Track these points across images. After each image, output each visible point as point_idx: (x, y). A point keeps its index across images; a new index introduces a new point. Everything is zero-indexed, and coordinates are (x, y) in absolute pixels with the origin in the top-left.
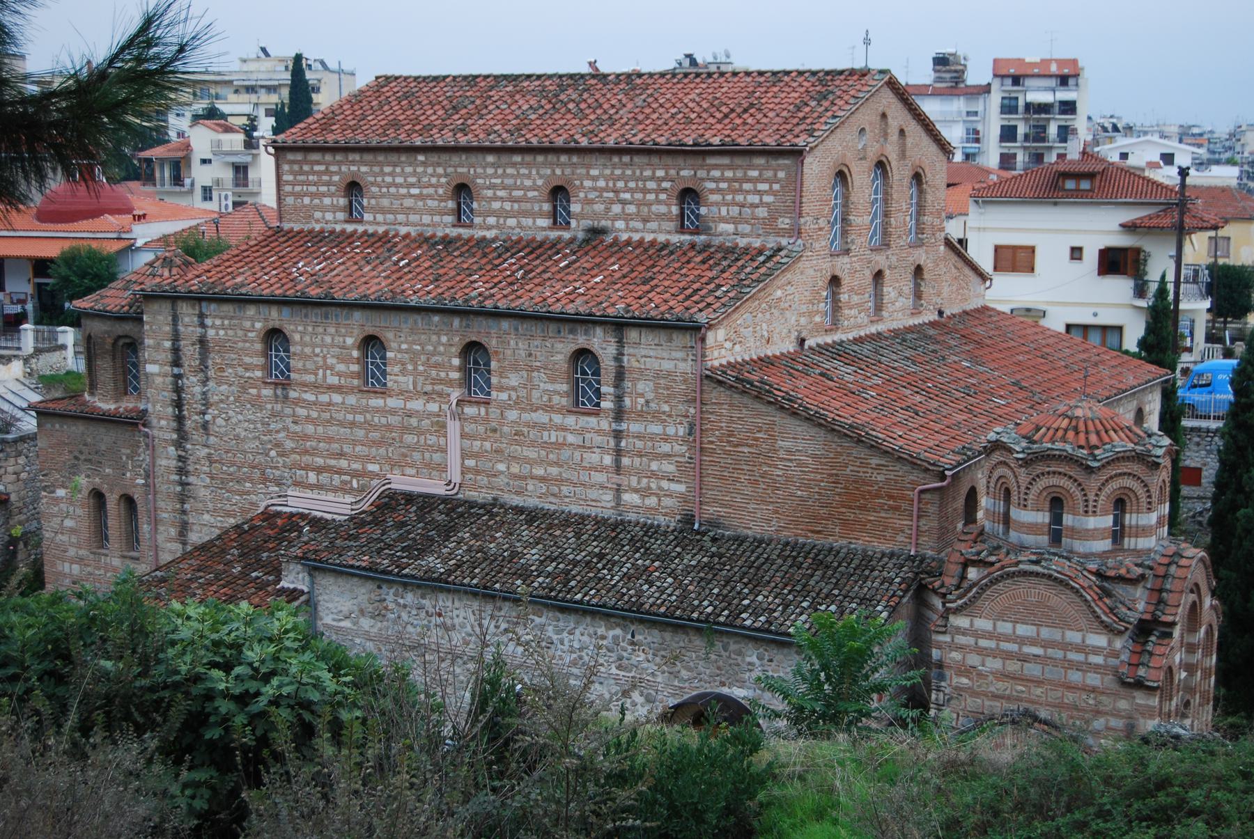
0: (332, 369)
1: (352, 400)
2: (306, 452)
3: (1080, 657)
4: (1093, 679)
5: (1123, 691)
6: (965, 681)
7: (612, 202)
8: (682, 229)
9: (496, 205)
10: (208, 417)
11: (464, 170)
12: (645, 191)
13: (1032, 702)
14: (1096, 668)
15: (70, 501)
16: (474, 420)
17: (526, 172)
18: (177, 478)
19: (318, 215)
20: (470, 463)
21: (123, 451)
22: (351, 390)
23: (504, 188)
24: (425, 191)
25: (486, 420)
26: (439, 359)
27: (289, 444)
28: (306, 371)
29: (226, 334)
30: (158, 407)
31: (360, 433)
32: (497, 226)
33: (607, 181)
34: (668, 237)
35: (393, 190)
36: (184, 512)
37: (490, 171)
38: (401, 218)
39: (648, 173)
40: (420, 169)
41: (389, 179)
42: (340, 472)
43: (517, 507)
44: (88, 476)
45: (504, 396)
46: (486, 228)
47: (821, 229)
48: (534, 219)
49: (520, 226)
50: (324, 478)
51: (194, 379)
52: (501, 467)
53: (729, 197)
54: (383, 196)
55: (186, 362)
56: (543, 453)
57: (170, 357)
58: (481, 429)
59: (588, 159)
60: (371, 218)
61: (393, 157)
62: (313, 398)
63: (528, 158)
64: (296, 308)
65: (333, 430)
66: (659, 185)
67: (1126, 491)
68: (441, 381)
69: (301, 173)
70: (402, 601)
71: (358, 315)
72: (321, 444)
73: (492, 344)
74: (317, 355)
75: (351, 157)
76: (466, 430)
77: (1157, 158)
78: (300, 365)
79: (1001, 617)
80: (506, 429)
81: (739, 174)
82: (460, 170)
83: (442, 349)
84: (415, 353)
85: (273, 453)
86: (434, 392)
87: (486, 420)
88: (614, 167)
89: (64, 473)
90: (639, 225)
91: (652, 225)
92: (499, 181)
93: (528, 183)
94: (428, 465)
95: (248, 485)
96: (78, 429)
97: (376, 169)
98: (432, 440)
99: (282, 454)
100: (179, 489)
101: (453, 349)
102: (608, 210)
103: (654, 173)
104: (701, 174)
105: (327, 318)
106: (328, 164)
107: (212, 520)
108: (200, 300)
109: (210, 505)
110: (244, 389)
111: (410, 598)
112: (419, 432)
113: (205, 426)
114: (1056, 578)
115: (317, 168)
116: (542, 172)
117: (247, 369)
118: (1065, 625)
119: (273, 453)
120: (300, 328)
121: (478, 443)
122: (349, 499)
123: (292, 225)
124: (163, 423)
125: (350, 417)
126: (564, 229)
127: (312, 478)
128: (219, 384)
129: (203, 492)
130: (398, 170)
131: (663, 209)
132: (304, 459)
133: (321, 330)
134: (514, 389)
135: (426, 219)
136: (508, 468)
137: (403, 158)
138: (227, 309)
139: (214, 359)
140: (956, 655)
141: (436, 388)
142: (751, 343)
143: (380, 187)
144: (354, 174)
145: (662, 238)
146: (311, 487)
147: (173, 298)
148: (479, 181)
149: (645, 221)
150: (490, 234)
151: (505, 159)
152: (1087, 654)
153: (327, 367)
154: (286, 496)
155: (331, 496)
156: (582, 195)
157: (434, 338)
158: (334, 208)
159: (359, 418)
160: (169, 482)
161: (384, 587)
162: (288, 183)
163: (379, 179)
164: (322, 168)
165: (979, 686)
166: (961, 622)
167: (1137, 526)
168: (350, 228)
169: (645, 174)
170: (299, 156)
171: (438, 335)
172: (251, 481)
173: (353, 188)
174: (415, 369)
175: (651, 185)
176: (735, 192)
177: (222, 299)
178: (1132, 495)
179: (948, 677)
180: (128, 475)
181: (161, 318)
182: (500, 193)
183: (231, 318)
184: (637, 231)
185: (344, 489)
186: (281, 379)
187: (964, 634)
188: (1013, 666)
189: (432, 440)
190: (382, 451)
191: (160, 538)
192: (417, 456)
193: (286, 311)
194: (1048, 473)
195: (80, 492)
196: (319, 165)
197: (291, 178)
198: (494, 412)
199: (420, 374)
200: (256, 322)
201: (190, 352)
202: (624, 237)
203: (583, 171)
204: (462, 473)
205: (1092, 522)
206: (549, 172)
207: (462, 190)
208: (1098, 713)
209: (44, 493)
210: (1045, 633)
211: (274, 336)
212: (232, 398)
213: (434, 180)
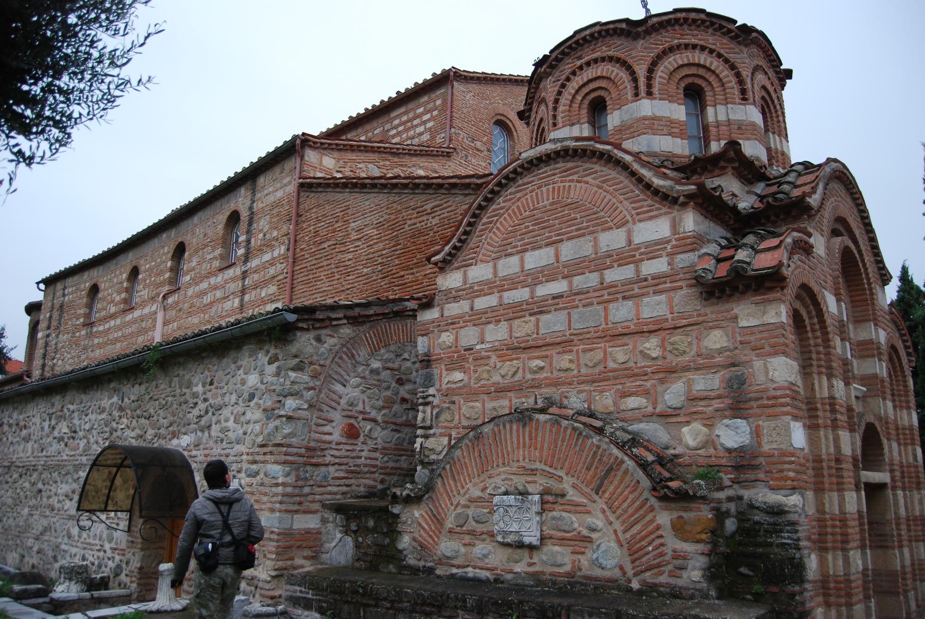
3: (628, 272)
4: (654, 307)
5: (711, 312)
6: (458, 376)
13: (556, 384)
14: (656, 283)
47: (478, 150)
53: (404, 136)
67: (701, 72)
79: (504, 251)
81: (411, 115)
104: (388, 126)
114: (575, 151)
118: (597, 223)
140: (446, 338)
152: (637, 263)
165: (479, 379)
166: (451, 280)
167: (729, 122)
176: (407, 130)
178: (712, 79)
179: (436, 377)
187: (456, 299)
188: (524, 328)
194: (581, 68)
205: (646, 107)
208: (670, 372)
210: (569, 251)
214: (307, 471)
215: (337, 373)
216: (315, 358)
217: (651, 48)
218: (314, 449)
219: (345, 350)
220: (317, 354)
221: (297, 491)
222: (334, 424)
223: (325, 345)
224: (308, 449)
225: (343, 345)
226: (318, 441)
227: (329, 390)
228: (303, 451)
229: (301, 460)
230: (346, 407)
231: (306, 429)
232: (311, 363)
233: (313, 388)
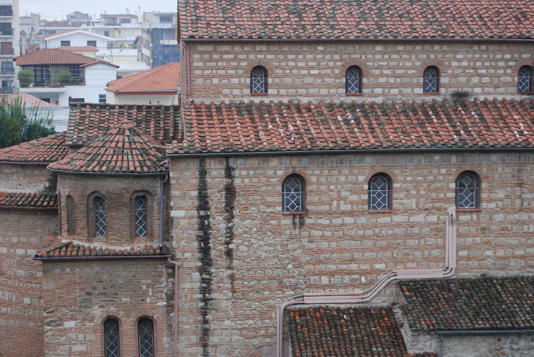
0: (345, 199)
1: (363, 220)
2: (321, 262)
7: (472, 76)
8: (520, 92)
9: (382, 80)
10: (231, 246)
11: (358, 56)
12: (496, 68)
15: (79, 330)
16: (467, 224)
17: (408, 57)
18: (201, 296)
19: (226, 91)
20: (464, 253)
21: (143, 281)
22: (363, 213)
23: (389, 68)
24: (323, 72)
25: (478, 222)
26: (438, 185)
27: (304, 259)
28: (322, 203)
29: (251, 181)
30: (183, 243)
31: (369, 243)
32: (383, 95)
33: (469, 60)
34: (513, 97)
35: (295, 71)
36: (206, 322)
37: (378, 57)
38: (301, 91)
39: (499, 56)
40: (319, 56)
41: (292, 64)
42: (350, 273)
43: (502, 277)
44: (103, 307)
45: (493, 205)
46: (373, 95)
48: (413, 88)
49: (401, 93)
50: (336, 279)
51: (221, 218)
52: (489, 253)
54: (287, 76)
55: (213, 205)
56: (523, 240)
57: (196, 203)
58: (473, 229)
59: (455, 48)
60: (275, 92)
61: (298, 48)
62: (328, 222)
63: (409, 48)
64: (313, 158)
65: (344, 244)
66: (506, 64)
68: (440, 200)
69: (211, 60)
70: (515, 347)
71: (369, 160)
72: (334, 255)
73: (483, 171)
74: (332, 191)
75: (258, 48)
76: (460, 231)
77: (85, 44)
78: (316, 199)
80: (493, 227)
82: (353, 56)
83: (441, 178)
84: (418, 182)
85: (290, 266)
86: (433, 208)
87: (478, 222)
88: (475, 52)
89: (73, 307)
90: (492, 90)
91: (502, 90)
92: (385, 63)
93: (408, 64)
94: (427, 259)
95: (266, 293)
96: (96, 268)
97: (281, 57)
98: (431, 241)
99: (299, 266)
100: (202, 304)
101: (451, 177)
102: (469, 81)
103: (503, 56)
105: (341, 163)
106: (236, 54)
107: (233, 324)
108: (227, 157)
109: (232, 313)
110: (265, 221)
111: (522, 343)
112: (420, 237)
113: (229, 253)
115: (225, 56)
116: (420, 56)
117: (268, 206)
119: (290, 266)
120: (316, 172)
121: (471, 239)
122: (357, 291)
123: (202, 100)
124: (187, 255)
125: (361, 233)
126: (436, 95)
127: (325, 280)
128: (242, 220)
129: (225, 304)
130: (301, 57)
131: (509, 79)
132: (318, 267)
133: (336, 172)
134: (501, 200)
135: (324, 91)
136: (495, 253)
137: (305, 48)
138: (254, 162)
139: (239, 201)
141: (436, 205)
143: (283, 69)
144: (260, 60)
145: (509, 98)
146: (324, 287)
147: (202, 157)
148: (368, 64)
149: (496, 87)
150: (379, 100)
151: (390, 48)
153: (340, 198)
154: (303, 296)
155: (342, 291)
156: (450, 71)
157: (435, 171)
158: (241, 86)
159: (369, 232)
160: (192, 300)
161: (503, 339)
162: (197, 68)
163: (283, 64)
164: (232, 56)
168: (257, 100)
169: (497, 57)
170: (210, 48)
171: (438, 168)
172: (270, 290)
173: (259, 71)
174: (418, 193)
175: (501, 64)
177: (248, 155)
180: (148, 300)
181: (189, 173)
182: (385, 72)
183: (256, 169)
184: (490, 94)
185: (354, 284)
186: (298, 213)
189: (431, 241)
190: (388, 254)
191: (181, 346)
192: (418, 254)
193: (305, 161)
195: (91, 321)
196: (228, 54)
197: (201, 64)
198: (484, 217)
199: (422, 197)
200: (278, 170)
201: (217, 199)
202: (482, 98)
203: (452, 56)
204: (457, 260)
206: (425, 56)
207: (355, 72)
209: (47, 327)
211: (295, 181)
212: (255, 229)
213: (331, 64)
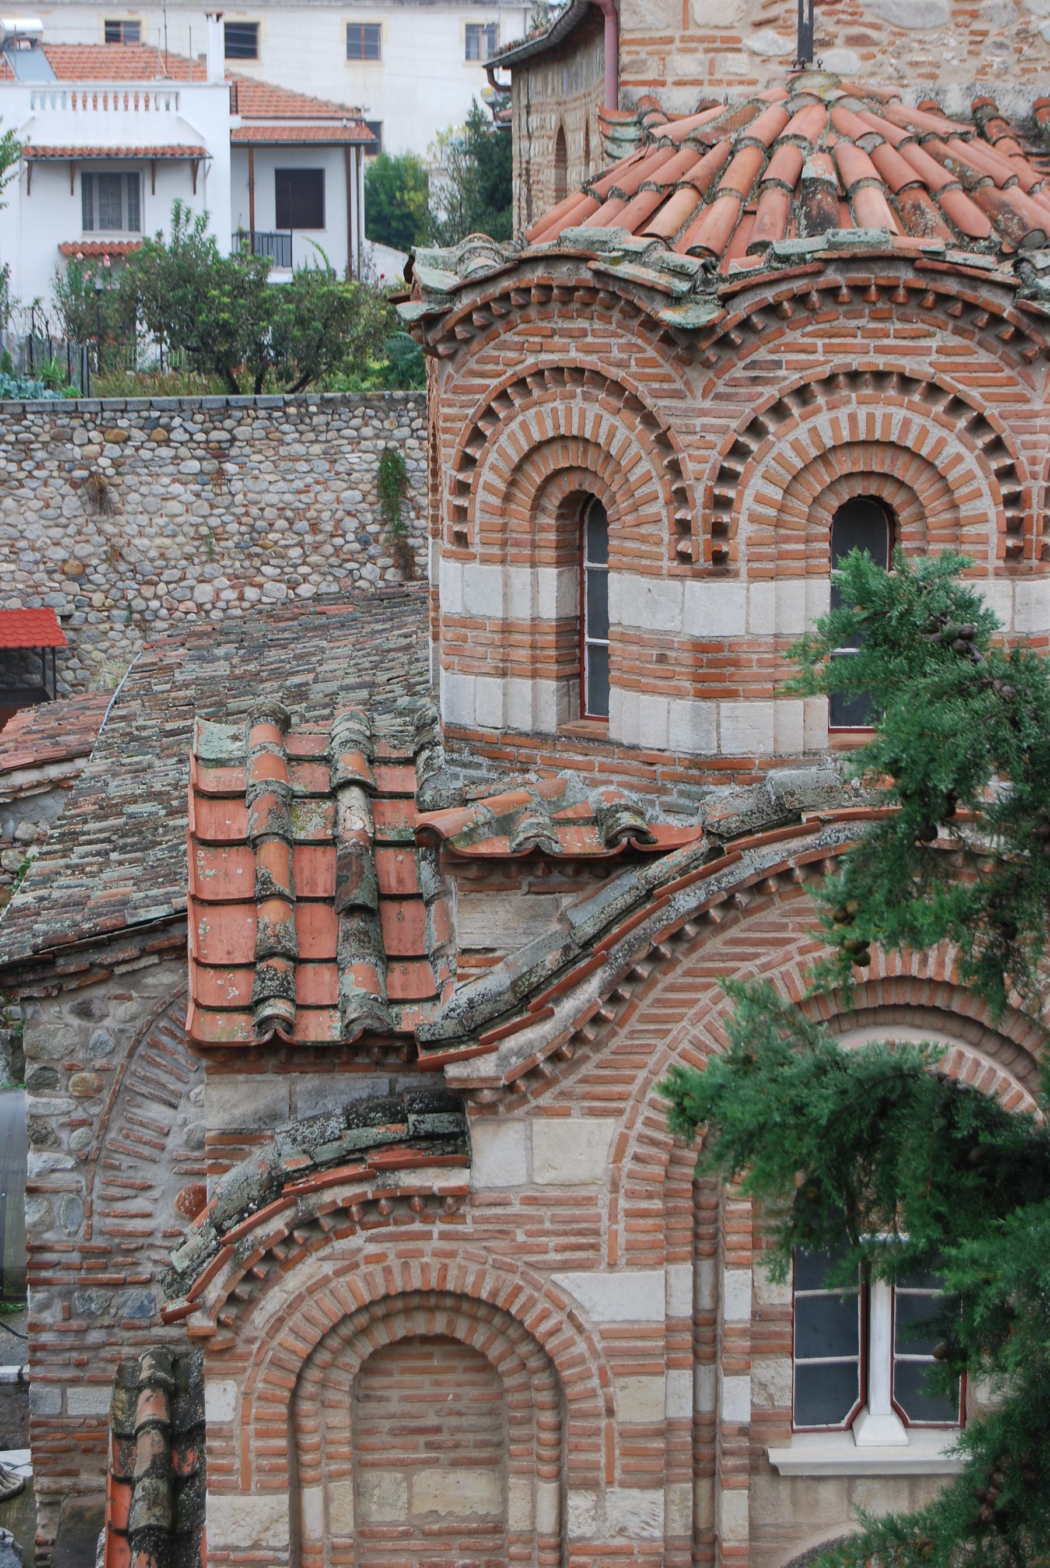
142: (952, 46)
214: (91, 1299)
215: (146, 1080)
216: (81, 1055)
217: (470, 390)
218: (105, 1252)
219: (162, 1024)
220: (84, 1045)
221: (70, 1340)
222: (155, 1193)
223: (107, 1022)
224: (87, 1253)
225: (158, 1015)
226: (112, 1234)
227: (130, 1120)
228: (75, 1257)
229: (71, 1276)
230: (183, 1152)
231: (78, 1212)
232: (71, 1069)
233: (81, 1123)
